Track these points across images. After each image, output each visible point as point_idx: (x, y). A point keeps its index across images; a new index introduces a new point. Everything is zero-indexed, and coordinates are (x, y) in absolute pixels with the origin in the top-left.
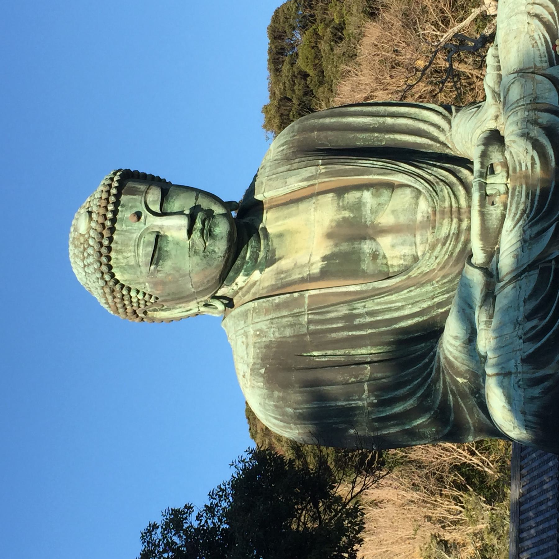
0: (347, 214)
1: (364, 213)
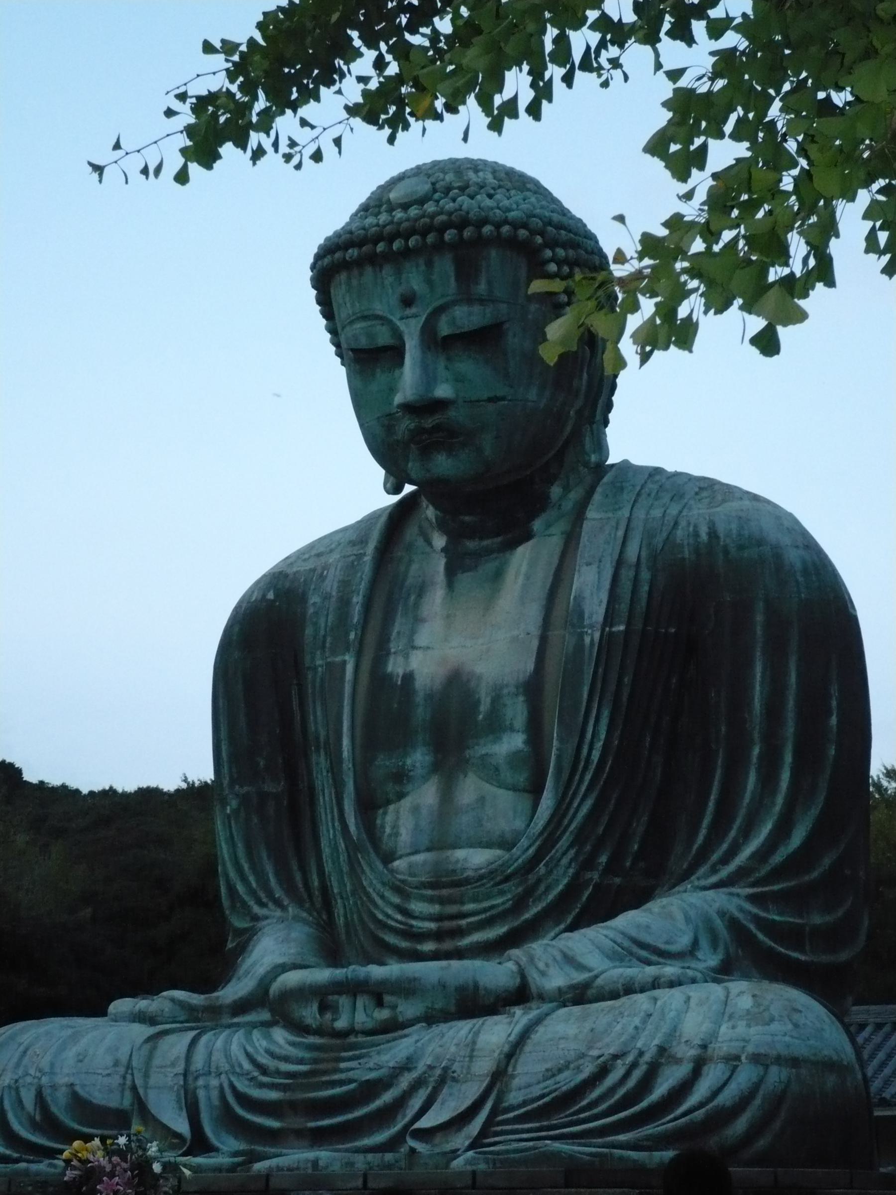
0: (485, 707)
1: (482, 741)
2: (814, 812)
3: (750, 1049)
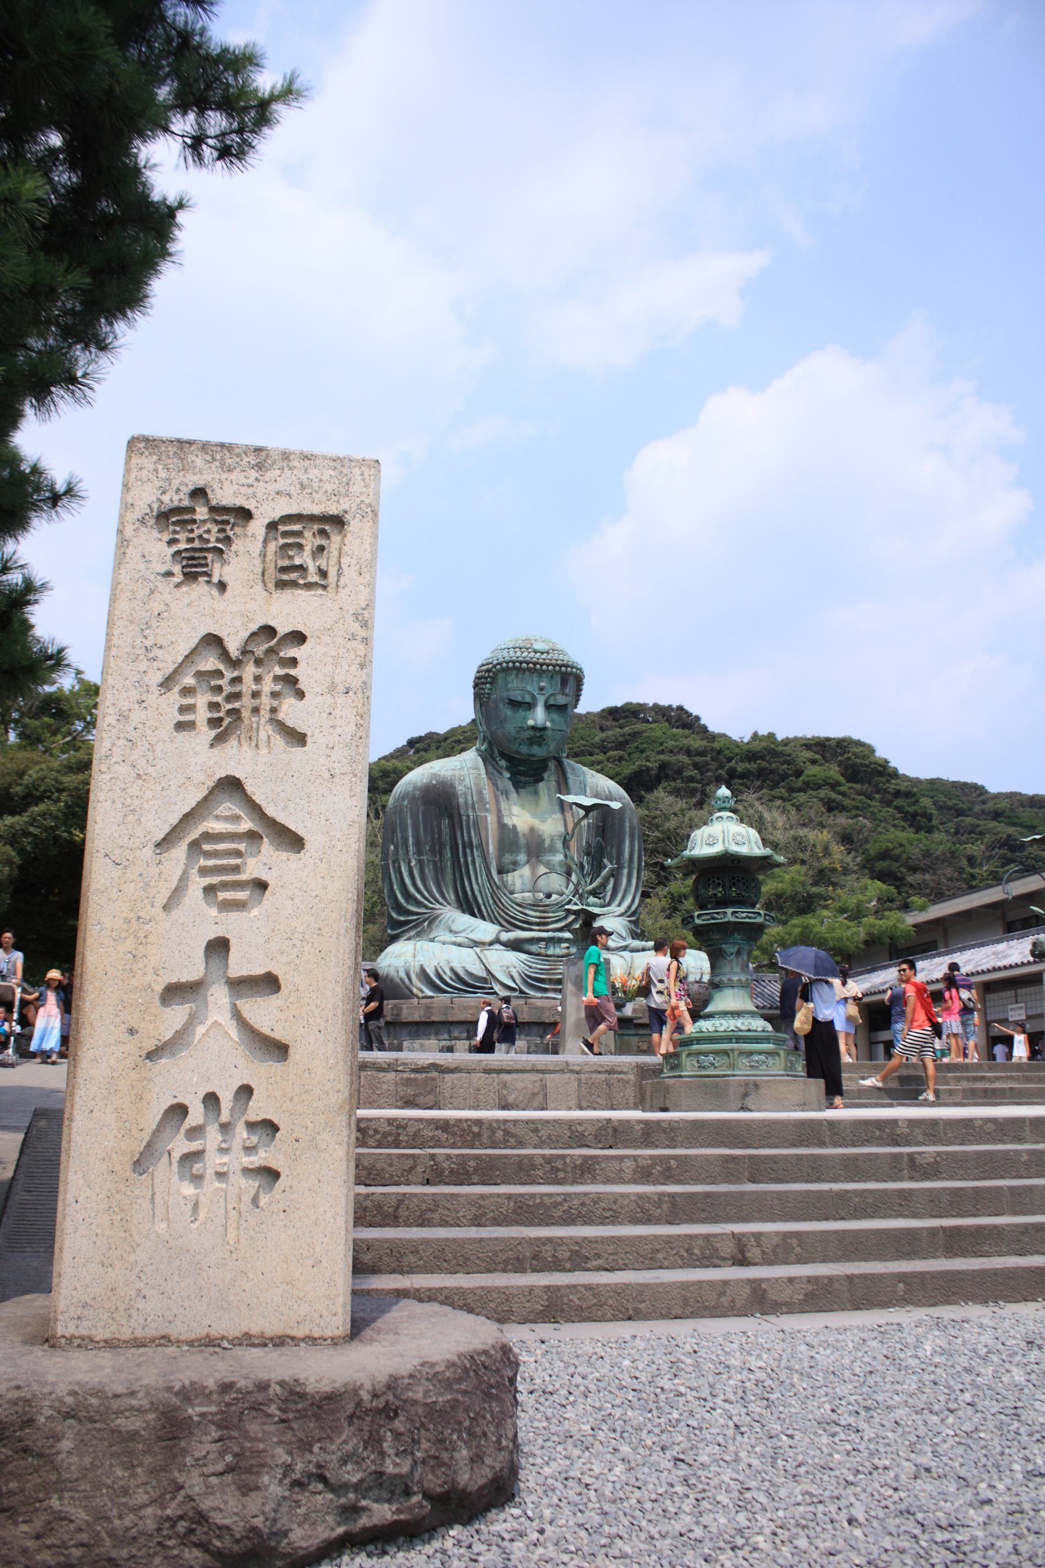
0: (547, 842)
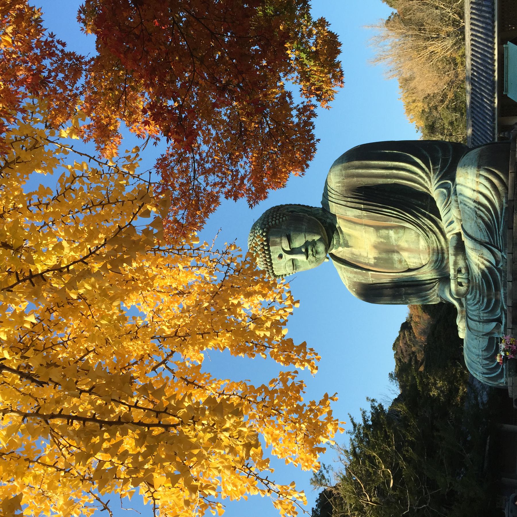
0: (382, 240)
2: (412, 156)
3: (475, 179)
